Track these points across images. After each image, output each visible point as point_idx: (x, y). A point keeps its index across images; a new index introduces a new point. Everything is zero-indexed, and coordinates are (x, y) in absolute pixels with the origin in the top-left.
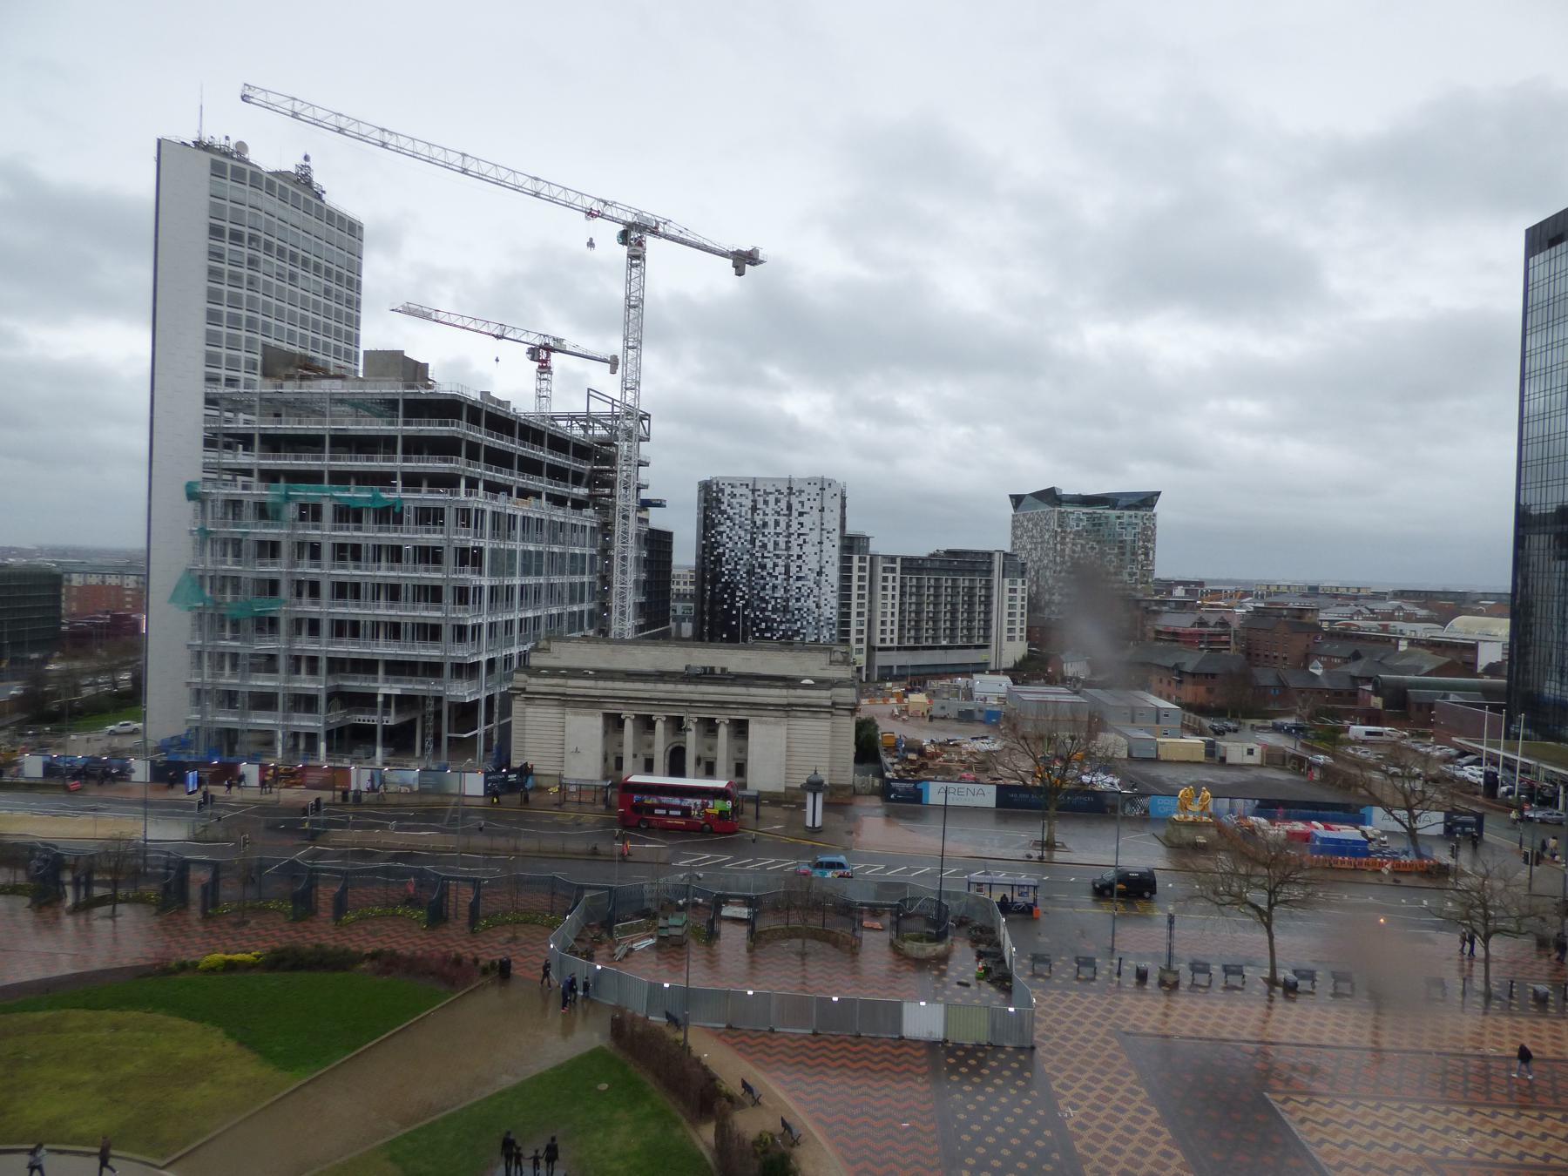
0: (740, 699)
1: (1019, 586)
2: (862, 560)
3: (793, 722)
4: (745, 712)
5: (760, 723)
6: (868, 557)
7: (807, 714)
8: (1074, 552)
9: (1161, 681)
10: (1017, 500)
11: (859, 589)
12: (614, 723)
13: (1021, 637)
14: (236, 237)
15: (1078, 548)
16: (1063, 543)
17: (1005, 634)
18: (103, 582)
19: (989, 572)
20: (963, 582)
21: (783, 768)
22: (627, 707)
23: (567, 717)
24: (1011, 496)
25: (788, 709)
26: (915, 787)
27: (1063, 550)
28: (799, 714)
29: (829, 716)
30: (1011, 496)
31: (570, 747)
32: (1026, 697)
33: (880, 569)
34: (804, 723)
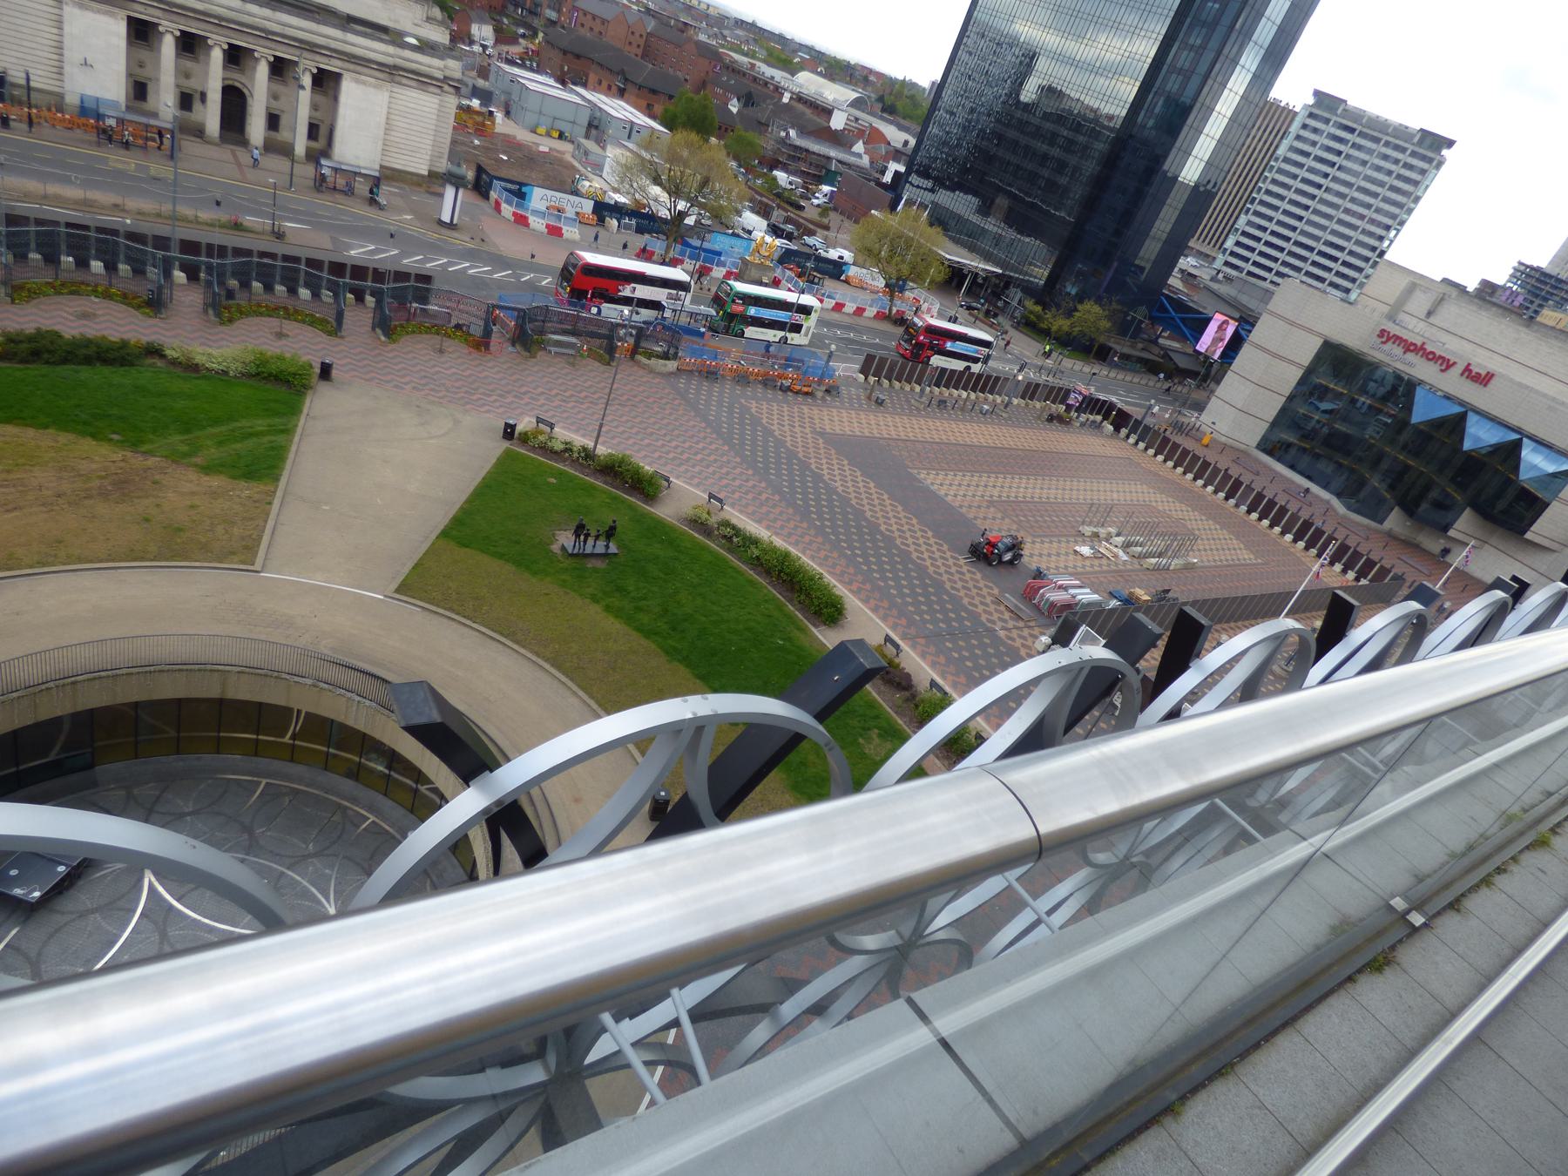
0: (333, 44)
3: (397, 89)
4: (339, 63)
5: (357, 81)
7: (413, 83)
9: (600, 83)
12: (141, 32)
21: (380, 143)
22: (167, 16)
23: (65, 7)
25: (392, 72)
26: (520, 189)
28: (404, 81)
29: (437, 91)
31: (73, 54)
32: (532, 86)
34: (409, 93)
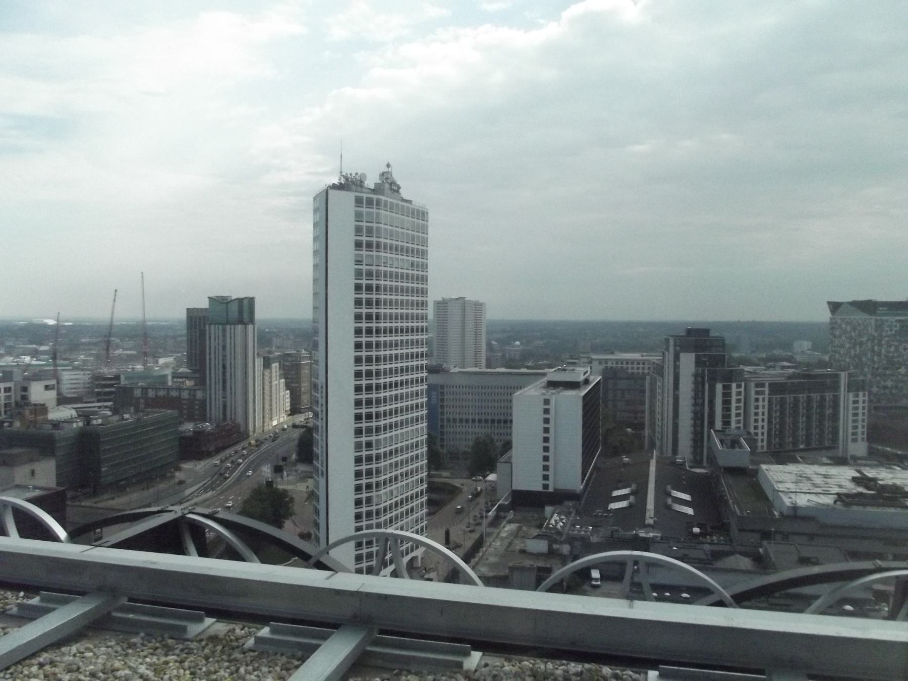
1: (861, 398)
2: (739, 386)
6: (743, 384)
8: (889, 352)
10: (835, 307)
11: (736, 410)
13: (863, 439)
14: (369, 245)
15: (892, 349)
16: (880, 345)
17: (850, 437)
18: (168, 393)
19: (835, 387)
20: (815, 396)
24: (829, 303)
27: (881, 350)
30: (829, 303)
33: (753, 392)
